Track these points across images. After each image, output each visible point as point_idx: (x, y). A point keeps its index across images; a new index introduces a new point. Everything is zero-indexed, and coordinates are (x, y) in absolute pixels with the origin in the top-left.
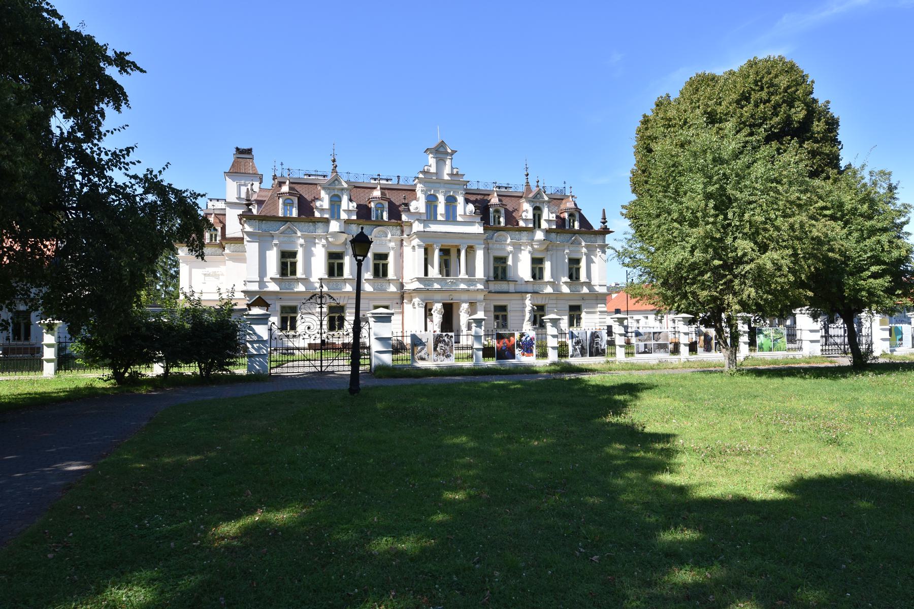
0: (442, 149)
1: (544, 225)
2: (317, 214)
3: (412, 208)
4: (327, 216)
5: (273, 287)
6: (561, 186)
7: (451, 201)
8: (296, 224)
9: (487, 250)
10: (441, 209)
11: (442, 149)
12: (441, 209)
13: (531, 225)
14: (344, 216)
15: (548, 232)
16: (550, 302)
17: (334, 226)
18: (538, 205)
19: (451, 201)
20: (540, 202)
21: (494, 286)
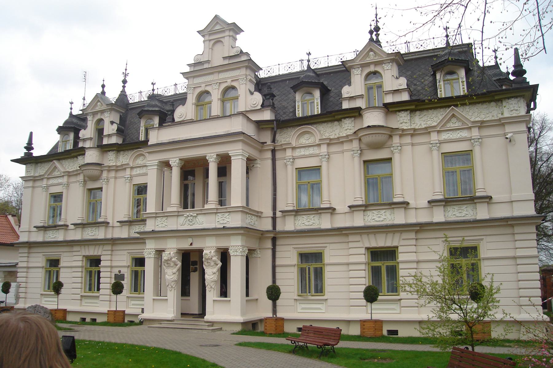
0: (218, 27)
2: (81, 145)
3: (177, 120)
4: (88, 144)
5: (38, 237)
7: (229, 92)
8: (64, 161)
10: (216, 110)
11: (218, 27)
12: (216, 110)
14: (105, 142)
15: (390, 109)
16: (403, 242)
17: (91, 156)
18: (372, 68)
19: (229, 92)
20: (376, 63)
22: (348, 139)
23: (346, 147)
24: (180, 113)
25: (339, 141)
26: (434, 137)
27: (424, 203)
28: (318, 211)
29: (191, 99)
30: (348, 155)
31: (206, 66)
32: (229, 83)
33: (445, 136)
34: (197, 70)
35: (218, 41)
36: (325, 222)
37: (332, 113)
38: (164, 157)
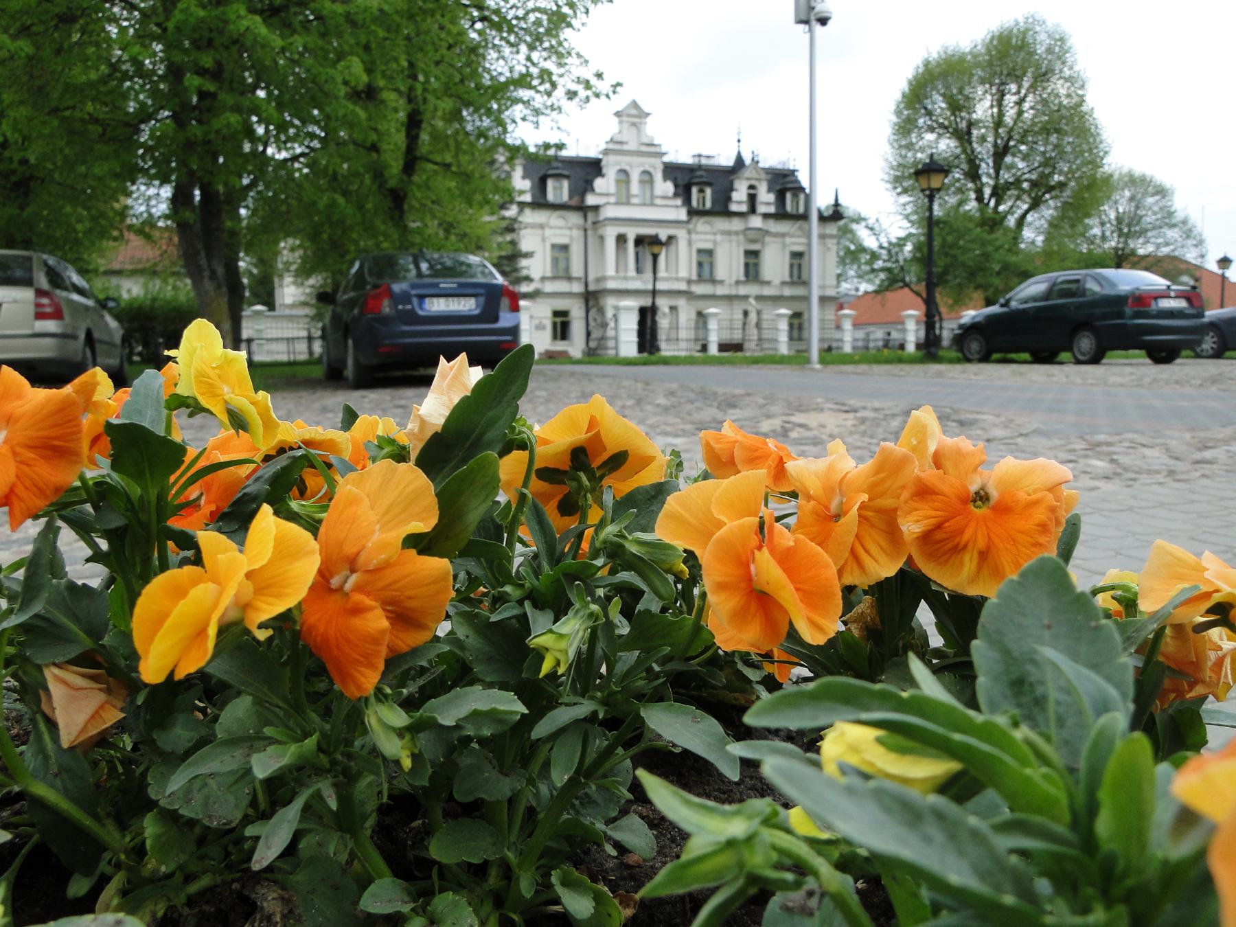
1: (762, 209)
6: (784, 159)
9: (690, 243)
10: (635, 188)
11: (634, 112)
13: (744, 208)
15: (766, 216)
18: (753, 182)
21: (699, 289)
22: (737, 233)
23: (734, 237)
24: (599, 184)
25: (729, 233)
26: (788, 240)
27: (777, 282)
28: (713, 281)
29: (611, 172)
30: (734, 244)
31: (626, 147)
32: (647, 168)
33: (794, 240)
34: (615, 147)
35: (634, 124)
36: (720, 291)
37: (722, 209)
38: (622, 230)
